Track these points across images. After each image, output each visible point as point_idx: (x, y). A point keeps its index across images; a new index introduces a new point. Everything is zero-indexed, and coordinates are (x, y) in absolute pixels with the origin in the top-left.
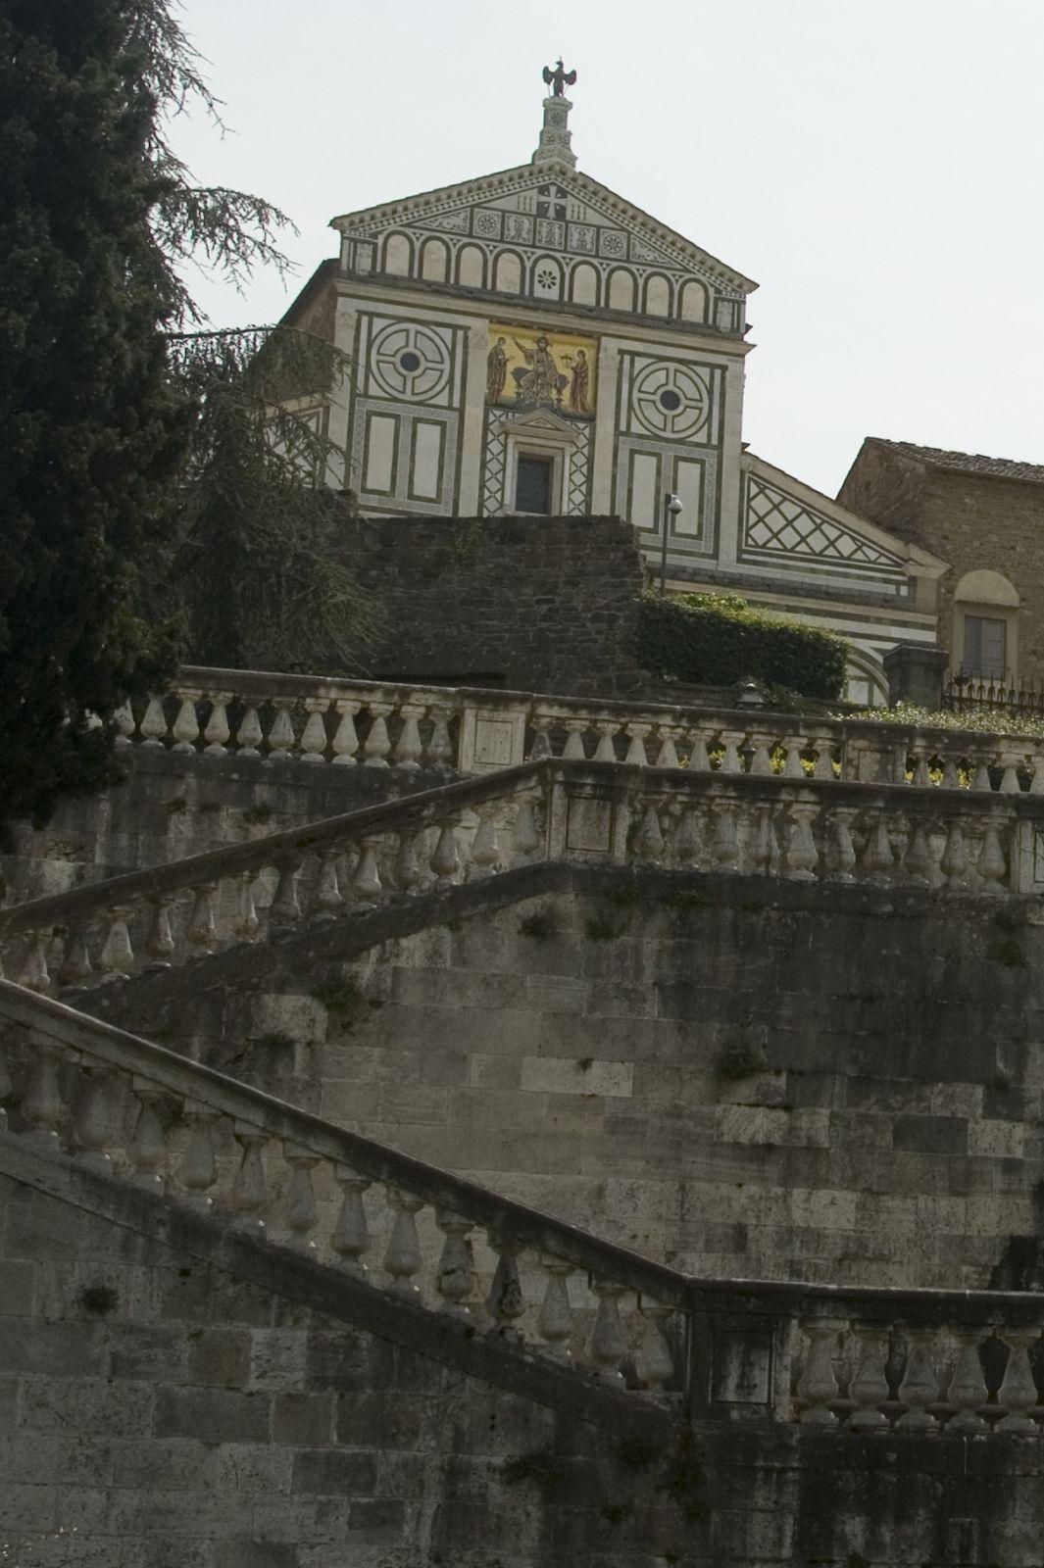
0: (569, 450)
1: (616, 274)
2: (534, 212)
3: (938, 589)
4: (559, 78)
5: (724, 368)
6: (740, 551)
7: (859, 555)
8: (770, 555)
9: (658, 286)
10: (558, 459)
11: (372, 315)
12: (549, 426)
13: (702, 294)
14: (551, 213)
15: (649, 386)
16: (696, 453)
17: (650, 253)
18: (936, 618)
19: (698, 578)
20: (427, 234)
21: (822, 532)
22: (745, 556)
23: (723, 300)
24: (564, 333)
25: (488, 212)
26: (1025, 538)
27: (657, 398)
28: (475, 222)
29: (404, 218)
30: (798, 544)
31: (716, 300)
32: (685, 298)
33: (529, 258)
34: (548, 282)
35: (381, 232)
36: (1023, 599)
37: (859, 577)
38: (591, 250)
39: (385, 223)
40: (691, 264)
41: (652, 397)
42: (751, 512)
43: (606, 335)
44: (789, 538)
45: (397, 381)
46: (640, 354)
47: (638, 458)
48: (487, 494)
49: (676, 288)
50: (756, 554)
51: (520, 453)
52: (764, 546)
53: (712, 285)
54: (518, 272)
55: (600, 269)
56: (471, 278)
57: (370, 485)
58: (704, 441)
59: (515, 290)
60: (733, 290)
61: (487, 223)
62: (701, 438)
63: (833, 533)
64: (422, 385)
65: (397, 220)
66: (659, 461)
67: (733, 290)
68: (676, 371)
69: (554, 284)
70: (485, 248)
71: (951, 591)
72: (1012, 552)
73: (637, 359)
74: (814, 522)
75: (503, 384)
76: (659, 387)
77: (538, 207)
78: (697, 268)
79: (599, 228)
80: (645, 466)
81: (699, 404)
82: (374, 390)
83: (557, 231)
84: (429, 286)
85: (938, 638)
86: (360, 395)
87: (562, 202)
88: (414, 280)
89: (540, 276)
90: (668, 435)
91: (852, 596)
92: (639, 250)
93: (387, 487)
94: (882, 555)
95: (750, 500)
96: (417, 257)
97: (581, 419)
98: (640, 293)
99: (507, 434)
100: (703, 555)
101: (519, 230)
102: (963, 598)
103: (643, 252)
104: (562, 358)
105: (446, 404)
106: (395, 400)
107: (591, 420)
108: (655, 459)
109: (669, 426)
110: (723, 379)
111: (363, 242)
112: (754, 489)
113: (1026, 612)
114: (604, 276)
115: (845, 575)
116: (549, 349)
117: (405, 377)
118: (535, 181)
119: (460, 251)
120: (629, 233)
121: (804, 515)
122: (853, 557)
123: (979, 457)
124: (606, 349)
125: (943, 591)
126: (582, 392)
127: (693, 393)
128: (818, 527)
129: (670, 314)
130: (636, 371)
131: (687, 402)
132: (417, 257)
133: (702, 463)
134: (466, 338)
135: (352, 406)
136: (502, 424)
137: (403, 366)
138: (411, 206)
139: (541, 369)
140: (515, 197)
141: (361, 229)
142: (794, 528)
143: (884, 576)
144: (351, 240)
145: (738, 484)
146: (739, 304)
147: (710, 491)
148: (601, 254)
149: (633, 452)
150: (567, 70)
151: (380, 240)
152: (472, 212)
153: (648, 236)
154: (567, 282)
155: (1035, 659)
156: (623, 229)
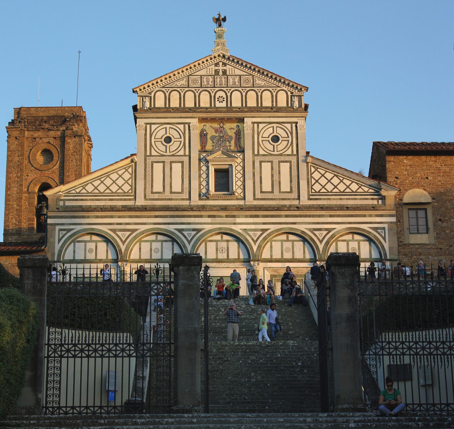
2: (214, 74)
4: (220, 21)
6: (309, 195)
7: (360, 190)
8: (322, 195)
9: (267, 95)
10: (230, 169)
11: (151, 124)
14: (221, 73)
16: (287, 158)
17: (262, 82)
18: (395, 211)
19: (292, 209)
20: (171, 89)
21: (343, 182)
22: (311, 197)
23: (294, 96)
25: (195, 77)
26: (432, 173)
27: (270, 139)
28: (190, 82)
29: (161, 85)
30: (334, 189)
31: (291, 96)
32: (278, 98)
33: (213, 92)
35: (153, 91)
36: (433, 199)
37: (361, 199)
38: (238, 85)
39: (154, 88)
41: (268, 139)
43: (246, 117)
44: (329, 187)
45: (163, 148)
46: (260, 123)
47: (262, 163)
48: (202, 187)
49: (274, 94)
50: (316, 195)
51: (215, 169)
52: (319, 192)
53: (289, 91)
55: (242, 92)
56: (190, 104)
57: (154, 191)
59: (208, 105)
60: (298, 91)
61: (195, 81)
62: (289, 152)
63: (348, 183)
65: (159, 86)
67: (298, 91)
68: (277, 127)
69: (224, 101)
70: (195, 91)
72: (426, 180)
73: (260, 125)
74: (340, 179)
76: (270, 134)
79: (240, 76)
80: (266, 167)
81: (287, 139)
82: (154, 153)
83: (223, 80)
85: (397, 220)
86: (148, 156)
87: (225, 68)
89: (218, 98)
90: (276, 153)
91: (358, 207)
92: (258, 82)
93: (162, 191)
94: (370, 188)
95: (311, 174)
96: (168, 99)
98: (259, 98)
100: (294, 199)
101: (208, 82)
102: (406, 202)
112: (313, 169)
113: (435, 204)
114: (244, 94)
115: (355, 199)
116: (224, 126)
120: (253, 76)
121: (335, 177)
122: (358, 191)
123: (422, 143)
124: (247, 123)
125: (398, 200)
126: (239, 141)
128: (341, 181)
129: (273, 105)
130: (260, 130)
132: (168, 99)
133: (290, 162)
135: (145, 160)
137: (165, 142)
139: (222, 135)
140: (206, 69)
141: (145, 92)
142: (331, 183)
143: (372, 197)
144: (140, 96)
145: (306, 168)
146: (300, 97)
147: (294, 173)
149: (261, 162)
150: (222, 17)
151: (153, 94)
152: (188, 78)
154: (229, 99)
155: (440, 223)
156: (250, 75)
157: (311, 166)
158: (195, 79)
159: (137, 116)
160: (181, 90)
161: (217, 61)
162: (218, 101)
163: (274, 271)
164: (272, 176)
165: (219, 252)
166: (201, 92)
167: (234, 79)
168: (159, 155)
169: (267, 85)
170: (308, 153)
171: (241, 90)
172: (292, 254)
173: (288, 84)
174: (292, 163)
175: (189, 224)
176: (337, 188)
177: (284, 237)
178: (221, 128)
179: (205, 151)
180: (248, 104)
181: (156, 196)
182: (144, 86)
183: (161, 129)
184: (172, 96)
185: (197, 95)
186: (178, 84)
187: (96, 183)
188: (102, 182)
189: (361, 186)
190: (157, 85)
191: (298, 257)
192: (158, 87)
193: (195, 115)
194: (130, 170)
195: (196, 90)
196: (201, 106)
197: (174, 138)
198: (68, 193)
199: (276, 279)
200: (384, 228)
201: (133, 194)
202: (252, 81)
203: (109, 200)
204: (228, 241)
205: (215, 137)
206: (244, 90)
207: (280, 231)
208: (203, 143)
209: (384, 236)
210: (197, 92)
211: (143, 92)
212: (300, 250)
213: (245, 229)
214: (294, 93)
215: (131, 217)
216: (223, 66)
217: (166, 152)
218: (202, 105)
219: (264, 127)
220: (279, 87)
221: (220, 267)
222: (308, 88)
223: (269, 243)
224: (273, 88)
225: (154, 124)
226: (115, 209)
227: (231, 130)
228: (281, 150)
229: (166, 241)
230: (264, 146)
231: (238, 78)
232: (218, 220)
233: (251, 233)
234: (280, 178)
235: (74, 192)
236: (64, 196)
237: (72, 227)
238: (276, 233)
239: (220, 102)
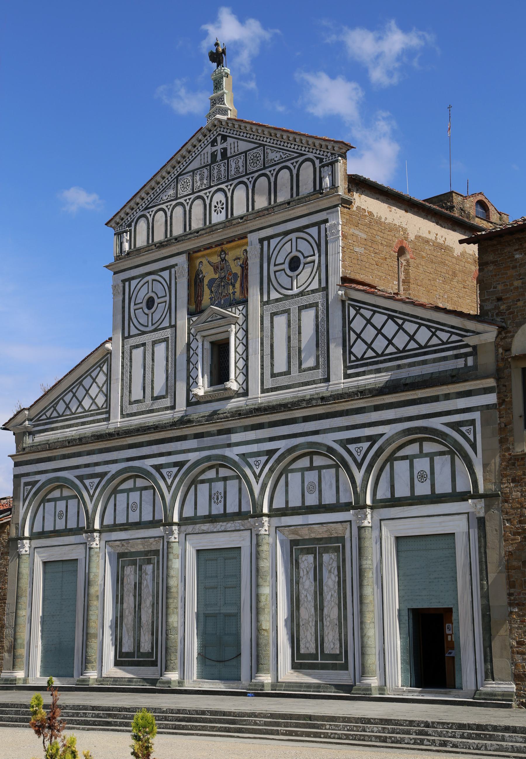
2: (210, 162)
3: (497, 350)
6: (346, 368)
7: (435, 341)
11: (129, 280)
12: (219, 317)
14: (219, 157)
19: (314, 403)
22: (349, 372)
23: (323, 166)
25: (185, 176)
30: (387, 347)
31: (320, 167)
35: (132, 221)
37: (435, 361)
38: (243, 171)
42: (351, 332)
43: (251, 232)
44: (380, 344)
45: (143, 319)
50: (357, 367)
52: (362, 358)
53: (317, 158)
57: (133, 399)
62: (315, 285)
63: (410, 327)
64: (156, 317)
66: (289, 314)
71: (508, 350)
79: (245, 152)
82: (134, 331)
85: (499, 398)
87: (224, 145)
89: (215, 207)
90: (296, 291)
93: (141, 398)
94: (452, 333)
95: (350, 322)
104: (235, 260)
106: (144, 333)
107: (245, 302)
112: (353, 312)
115: (424, 362)
116: (226, 258)
117: (147, 315)
119: (172, 212)
120: (264, 146)
122: (429, 344)
125: (501, 350)
135: (123, 346)
138: (143, 194)
140: (199, 156)
143: (455, 352)
145: (340, 313)
157: (349, 304)
162: (215, 211)
163: (295, 533)
164: (289, 338)
165: (213, 501)
166: (192, 202)
167: (237, 162)
169: (283, 157)
170: (345, 280)
172: (317, 496)
175: (169, 454)
176: (393, 345)
177: (305, 462)
181: (135, 408)
182: (120, 214)
183: (142, 286)
187: (67, 398)
188: (74, 395)
189: (436, 331)
191: (327, 503)
194: (105, 368)
198: (38, 420)
199: (298, 549)
200: (472, 422)
201: (108, 409)
203: (80, 424)
204: (225, 479)
207: (294, 452)
208: (198, 297)
209: (473, 440)
211: (122, 225)
212: (331, 485)
213: (244, 454)
215: (101, 451)
216: (223, 141)
220: (302, 155)
221: (215, 530)
223: (283, 478)
225: (133, 278)
226: (84, 441)
227: (236, 261)
228: (303, 284)
229: (146, 488)
231: (242, 157)
232: (207, 441)
233: (251, 460)
234: (300, 341)
235: (44, 417)
236: (35, 426)
237: (37, 477)
238: (288, 455)
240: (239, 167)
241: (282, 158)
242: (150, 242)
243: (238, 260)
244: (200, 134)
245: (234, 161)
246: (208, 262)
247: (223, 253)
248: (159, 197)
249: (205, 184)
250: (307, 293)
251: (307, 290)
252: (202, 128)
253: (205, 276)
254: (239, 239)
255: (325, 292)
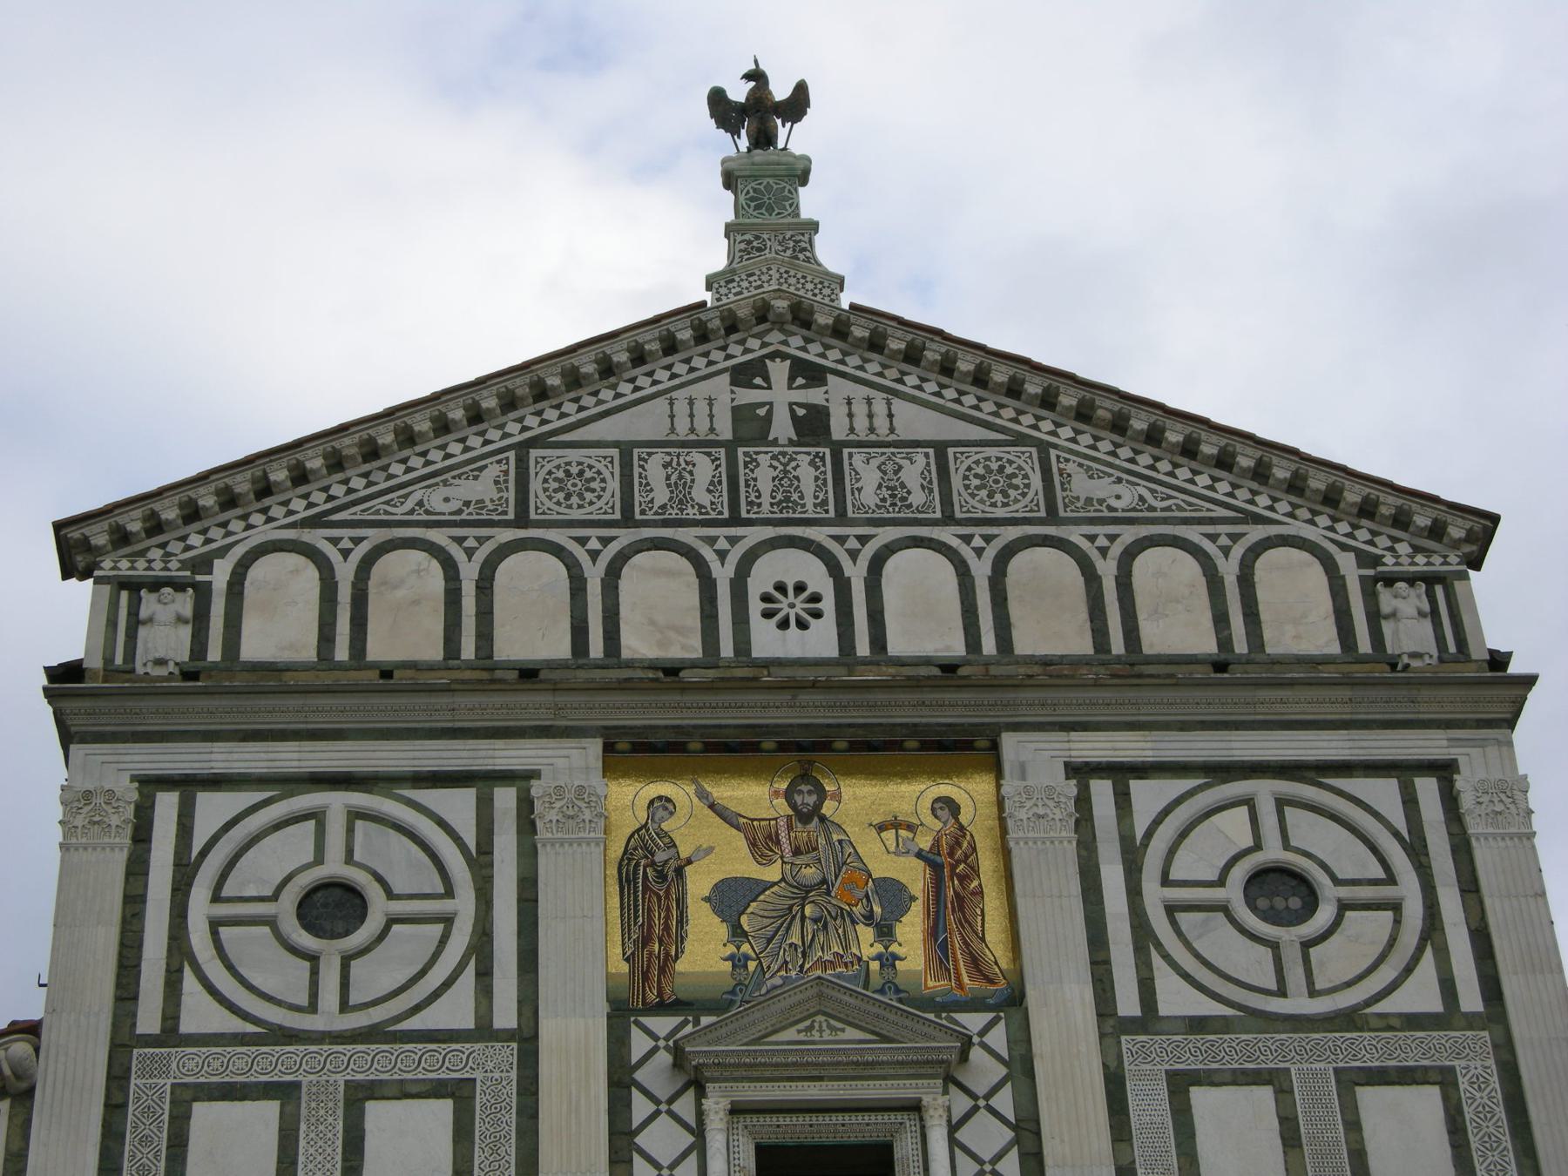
0: (939, 1104)
1: (1019, 564)
2: (726, 433)
5: (1444, 770)
10: (905, 1149)
11: (189, 785)
13: (1316, 575)
14: (782, 428)
15: (1196, 861)
16: (1412, 1050)
17: (1119, 489)
20: (376, 536)
23: (1390, 581)
24: (870, 747)
25: (573, 455)
27: (1233, 892)
28: (535, 485)
29: (298, 505)
32: (1262, 594)
33: (722, 555)
34: (800, 607)
35: (223, 552)
38: (927, 506)
39: (237, 526)
40: (1263, 500)
43: (1016, 727)
47: (1200, 1097)
49: (1229, 570)
51: (762, 1151)
53: (1344, 547)
54: (693, 598)
55: (967, 552)
58: (1435, 1005)
59: (689, 647)
60: (1417, 549)
61: (574, 483)
62: (1421, 995)
65: (276, 512)
66: (1283, 1092)
67: (1417, 549)
68: (1281, 803)
69: (817, 615)
73: (1136, 786)
75: (682, 939)
77: (735, 420)
78: (1283, 507)
79: (941, 448)
82: (199, 1014)
83: (806, 474)
84: (387, 674)
87: (815, 396)
88: (340, 667)
89: (766, 598)
90: (1298, 1004)
92: (1082, 485)
97: (975, 1004)
99: (697, 1085)
101: (680, 487)
103: (1102, 488)
104: (881, 828)
105: (469, 1023)
107: (1013, 1001)
108: (1265, 1094)
109: (1295, 975)
110: (1450, 800)
111: (155, 585)
114: (981, 570)
116: (828, 808)
117: (313, 959)
118: (717, 355)
120: (1043, 448)
126: (965, 922)
127: (1352, 860)
129: (1225, 643)
131: (1345, 892)
133: (1445, 1080)
134: (526, 806)
135: (117, 1078)
136: (679, 1057)
139: (810, 874)
140: (661, 404)
148: (958, 515)
149: (1180, 1084)
153: (1105, 446)
156: (1020, 440)
158: (574, 470)
159: (76, 723)
160: (460, 540)
161: (747, 351)
166: (622, 558)
167: (890, 467)
168: (251, 1028)
171: (955, 543)
173: (1331, 499)
174: (1463, 1083)
178: (804, 816)
179: (663, 1007)
180: (1015, 634)
182: (156, 506)
183: (278, 826)
184: (384, 583)
185: (594, 576)
186: (437, 500)
190: (265, 511)
192: (270, 520)
193: (578, 708)
195: (582, 541)
196: (626, 654)
197: (391, 895)
202: (1036, 481)
205: (756, 888)
206: (978, 542)
208: (646, 941)
210: (594, 555)
214: (1389, 559)
217: (312, 1007)
218: (637, 644)
219: (1178, 801)
220: (1258, 519)
222: (1495, 519)
224: (1210, 529)
225: (217, 782)
227: (889, 835)
228: (1349, 984)
230: (1197, 956)
231: (920, 460)
239: (784, 625)
240: (903, 486)
241: (1153, 509)
242: (342, 653)
243: (903, 833)
244: (688, 322)
245: (875, 463)
246: (712, 806)
247: (804, 788)
248: (406, 496)
249: (701, 507)
250: (1374, 1023)
251: (1379, 1008)
252: (704, 304)
253: (689, 862)
254: (925, 746)
255: (1485, 1034)
